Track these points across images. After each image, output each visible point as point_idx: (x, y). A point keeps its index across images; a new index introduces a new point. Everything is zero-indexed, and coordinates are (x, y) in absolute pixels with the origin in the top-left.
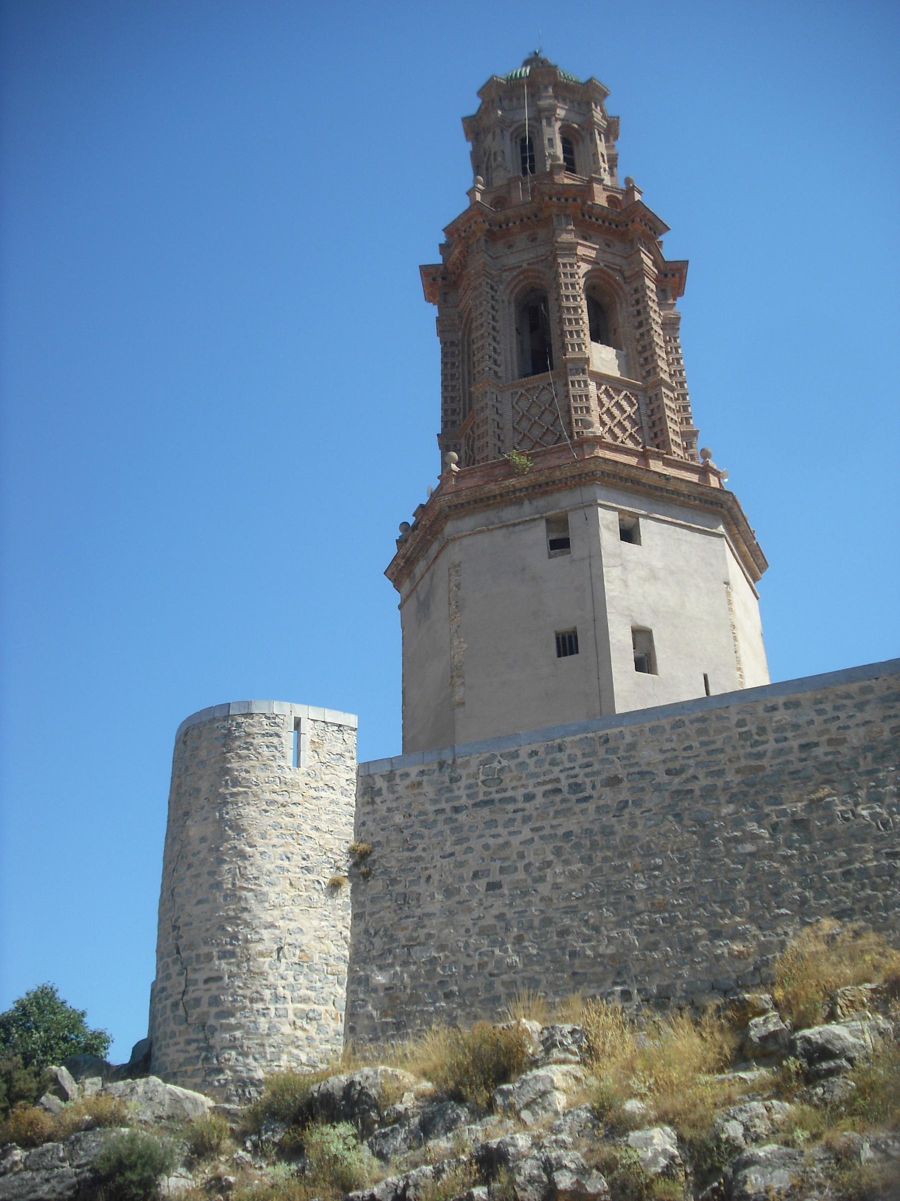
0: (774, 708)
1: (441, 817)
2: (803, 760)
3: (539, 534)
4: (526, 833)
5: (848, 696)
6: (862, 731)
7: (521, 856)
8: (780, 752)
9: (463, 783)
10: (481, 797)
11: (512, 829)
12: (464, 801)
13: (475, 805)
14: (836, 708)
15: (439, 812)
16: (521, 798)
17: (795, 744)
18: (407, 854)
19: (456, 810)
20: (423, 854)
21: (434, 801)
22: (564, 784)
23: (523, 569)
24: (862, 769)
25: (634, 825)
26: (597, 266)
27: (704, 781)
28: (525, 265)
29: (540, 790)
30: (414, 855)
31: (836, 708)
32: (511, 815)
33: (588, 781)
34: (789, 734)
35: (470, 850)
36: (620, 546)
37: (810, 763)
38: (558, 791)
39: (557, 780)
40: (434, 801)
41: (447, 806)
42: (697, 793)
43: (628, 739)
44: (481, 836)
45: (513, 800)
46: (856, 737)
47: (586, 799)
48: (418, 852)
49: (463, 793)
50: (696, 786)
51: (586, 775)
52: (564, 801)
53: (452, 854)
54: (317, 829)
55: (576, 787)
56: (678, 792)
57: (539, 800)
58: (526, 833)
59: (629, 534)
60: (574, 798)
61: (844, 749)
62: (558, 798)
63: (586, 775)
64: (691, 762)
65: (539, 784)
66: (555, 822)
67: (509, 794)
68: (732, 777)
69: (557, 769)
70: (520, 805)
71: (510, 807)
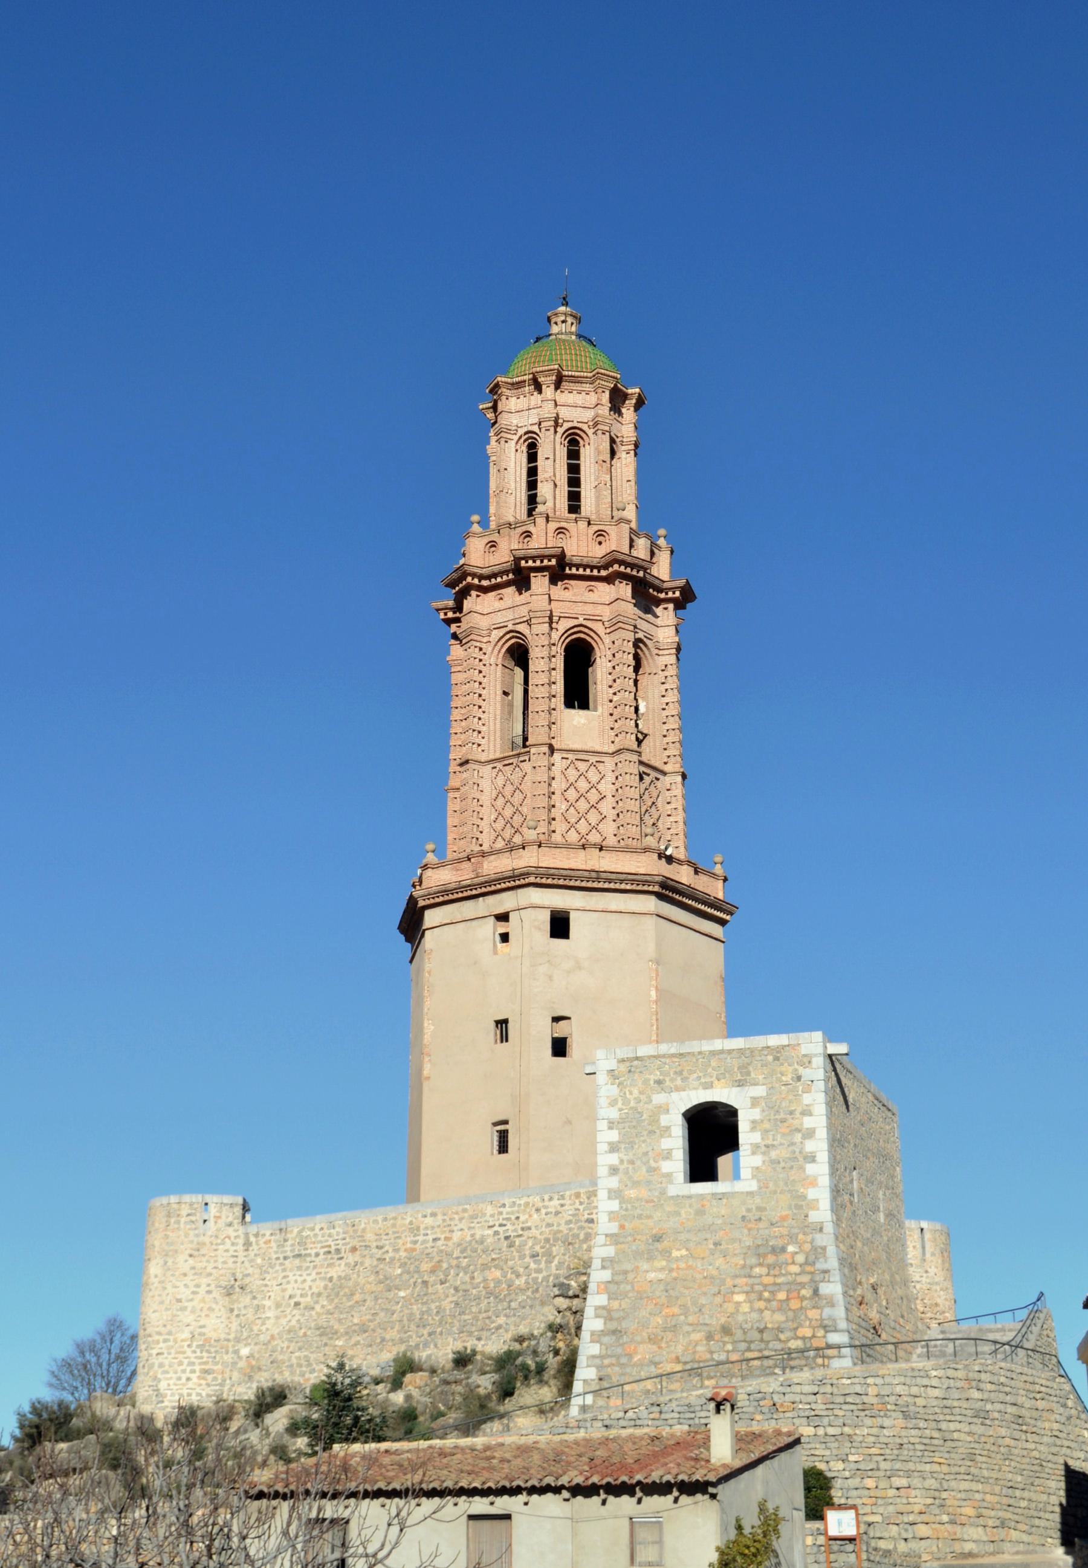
0: (425, 1216)
1: (278, 1262)
2: (433, 1247)
3: (490, 929)
4: (314, 1276)
5: (457, 1213)
6: (460, 1233)
7: (310, 1288)
8: (424, 1242)
9: (289, 1243)
10: (297, 1252)
11: (308, 1272)
12: (289, 1254)
13: (294, 1256)
14: (451, 1219)
15: (278, 1259)
16: (313, 1255)
17: (430, 1237)
18: (261, 1282)
19: (285, 1258)
20: (268, 1283)
21: (276, 1252)
22: (333, 1249)
23: (475, 963)
24: (454, 1256)
25: (359, 1276)
26: (576, 622)
27: (391, 1254)
28: (510, 627)
29: (322, 1251)
30: (264, 1282)
31: (451, 1219)
32: (308, 1264)
33: (343, 1248)
34: (429, 1232)
35: (288, 1283)
36: (548, 944)
37: (435, 1249)
38: (329, 1252)
39: (330, 1246)
40: (276, 1252)
41: (281, 1256)
42: (388, 1260)
43: (363, 1226)
44: (294, 1275)
45: (310, 1255)
46: (456, 1236)
47: (341, 1258)
48: (266, 1282)
49: (288, 1249)
50: (387, 1257)
51: (343, 1245)
52: (332, 1258)
53: (281, 1284)
54: (215, 1268)
55: (338, 1251)
56: (379, 1259)
57: (322, 1257)
58: (314, 1276)
59: (560, 926)
60: (336, 1257)
61: (450, 1243)
62: (329, 1256)
63: (343, 1245)
64: (387, 1242)
65: (322, 1247)
66: (326, 1270)
67: (309, 1251)
68: (403, 1254)
69: (331, 1239)
70: (313, 1259)
71: (308, 1259)
